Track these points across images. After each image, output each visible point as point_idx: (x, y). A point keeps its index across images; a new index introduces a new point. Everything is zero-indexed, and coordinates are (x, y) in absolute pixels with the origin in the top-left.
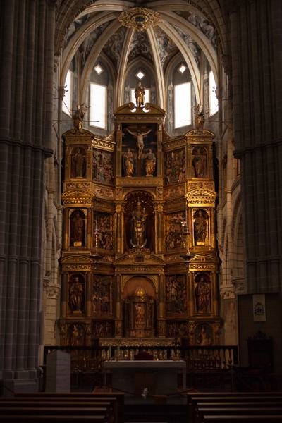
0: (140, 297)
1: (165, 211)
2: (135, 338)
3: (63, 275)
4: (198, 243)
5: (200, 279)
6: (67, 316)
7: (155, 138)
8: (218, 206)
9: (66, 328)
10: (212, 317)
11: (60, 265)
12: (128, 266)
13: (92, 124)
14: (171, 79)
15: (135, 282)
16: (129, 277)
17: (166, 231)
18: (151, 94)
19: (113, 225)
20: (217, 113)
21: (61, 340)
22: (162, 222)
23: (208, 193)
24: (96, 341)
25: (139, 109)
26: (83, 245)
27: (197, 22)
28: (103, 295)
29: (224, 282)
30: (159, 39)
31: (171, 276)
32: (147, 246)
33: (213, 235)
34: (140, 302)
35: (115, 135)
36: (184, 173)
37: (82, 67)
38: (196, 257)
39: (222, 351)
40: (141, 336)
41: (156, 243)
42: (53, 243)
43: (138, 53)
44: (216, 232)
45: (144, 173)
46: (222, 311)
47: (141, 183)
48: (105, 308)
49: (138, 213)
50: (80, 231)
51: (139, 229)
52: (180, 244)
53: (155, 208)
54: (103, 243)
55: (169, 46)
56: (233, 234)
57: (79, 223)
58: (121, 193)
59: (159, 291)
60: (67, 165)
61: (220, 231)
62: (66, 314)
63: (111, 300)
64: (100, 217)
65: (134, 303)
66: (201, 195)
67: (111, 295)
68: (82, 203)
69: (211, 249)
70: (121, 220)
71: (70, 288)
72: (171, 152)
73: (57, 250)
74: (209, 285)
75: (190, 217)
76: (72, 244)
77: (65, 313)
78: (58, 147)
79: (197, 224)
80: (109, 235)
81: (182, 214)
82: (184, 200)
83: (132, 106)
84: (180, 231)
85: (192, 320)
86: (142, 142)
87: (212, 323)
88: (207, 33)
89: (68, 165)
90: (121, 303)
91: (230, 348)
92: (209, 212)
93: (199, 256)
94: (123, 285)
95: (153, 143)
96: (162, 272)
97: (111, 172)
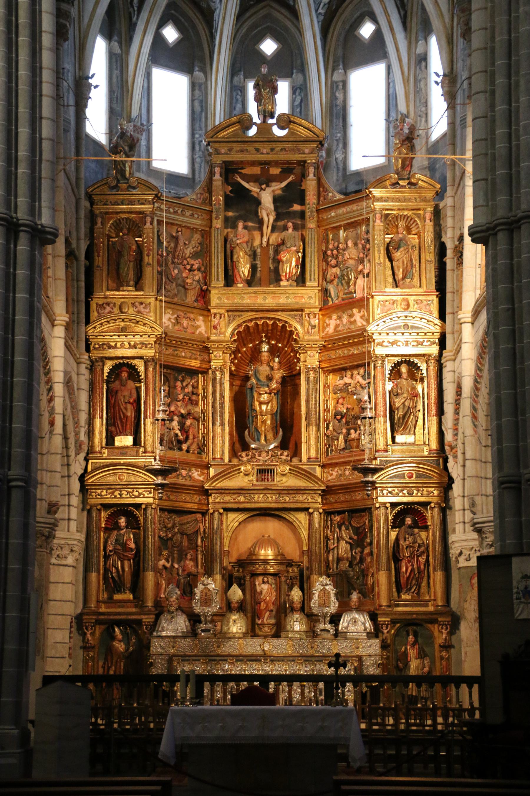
0: (266, 562)
1: (324, 365)
3: (89, 512)
4: (399, 438)
5: (403, 522)
6: (98, 607)
9: (98, 634)
12: (240, 491)
13: (156, 164)
14: (340, 52)
16: (241, 517)
17: (327, 410)
18: (294, 90)
19: (205, 397)
20: (444, 135)
21: (85, 662)
22: (317, 392)
23: (422, 324)
25: (264, 128)
26: (137, 442)
28: (181, 557)
29: (459, 528)
33: (434, 420)
34: (265, 574)
35: (209, 188)
36: (368, 275)
37: (132, 27)
38: (391, 471)
42: (66, 438)
44: (440, 412)
49: (264, 370)
50: (130, 413)
52: (359, 440)
53: (302, 357)
54: (181, 437)
56: (474, 417)
57: (126, 393)
58: (223, 323)
59: (310, 548)
61: (449, 408)
62: (98, 601)
64: (176, 379)
65: (254, 575)
66: (406, 326)
67: (200, 557)
68: (135, 347)
70: (222, 385)
71: (106, 542)
72: (338, 228)
74: (423, 534)
75: (379, 377)
76: (110, 442)
77: (94, 599)
78: (78, 219)
79: (397, 395)
80: (197, 419)
81: (362, 371)
82: (370, 340)
83: (247, 123)
85: (386, 615)
86: (272, 207)
87: (434, 621)
89: (100, 260)
90: (223, 576)
91: (470, 681)
92: (423, 367)
93: (402, 469)
94: (227, 535)
95: (297, 207)
97: (198, 276)
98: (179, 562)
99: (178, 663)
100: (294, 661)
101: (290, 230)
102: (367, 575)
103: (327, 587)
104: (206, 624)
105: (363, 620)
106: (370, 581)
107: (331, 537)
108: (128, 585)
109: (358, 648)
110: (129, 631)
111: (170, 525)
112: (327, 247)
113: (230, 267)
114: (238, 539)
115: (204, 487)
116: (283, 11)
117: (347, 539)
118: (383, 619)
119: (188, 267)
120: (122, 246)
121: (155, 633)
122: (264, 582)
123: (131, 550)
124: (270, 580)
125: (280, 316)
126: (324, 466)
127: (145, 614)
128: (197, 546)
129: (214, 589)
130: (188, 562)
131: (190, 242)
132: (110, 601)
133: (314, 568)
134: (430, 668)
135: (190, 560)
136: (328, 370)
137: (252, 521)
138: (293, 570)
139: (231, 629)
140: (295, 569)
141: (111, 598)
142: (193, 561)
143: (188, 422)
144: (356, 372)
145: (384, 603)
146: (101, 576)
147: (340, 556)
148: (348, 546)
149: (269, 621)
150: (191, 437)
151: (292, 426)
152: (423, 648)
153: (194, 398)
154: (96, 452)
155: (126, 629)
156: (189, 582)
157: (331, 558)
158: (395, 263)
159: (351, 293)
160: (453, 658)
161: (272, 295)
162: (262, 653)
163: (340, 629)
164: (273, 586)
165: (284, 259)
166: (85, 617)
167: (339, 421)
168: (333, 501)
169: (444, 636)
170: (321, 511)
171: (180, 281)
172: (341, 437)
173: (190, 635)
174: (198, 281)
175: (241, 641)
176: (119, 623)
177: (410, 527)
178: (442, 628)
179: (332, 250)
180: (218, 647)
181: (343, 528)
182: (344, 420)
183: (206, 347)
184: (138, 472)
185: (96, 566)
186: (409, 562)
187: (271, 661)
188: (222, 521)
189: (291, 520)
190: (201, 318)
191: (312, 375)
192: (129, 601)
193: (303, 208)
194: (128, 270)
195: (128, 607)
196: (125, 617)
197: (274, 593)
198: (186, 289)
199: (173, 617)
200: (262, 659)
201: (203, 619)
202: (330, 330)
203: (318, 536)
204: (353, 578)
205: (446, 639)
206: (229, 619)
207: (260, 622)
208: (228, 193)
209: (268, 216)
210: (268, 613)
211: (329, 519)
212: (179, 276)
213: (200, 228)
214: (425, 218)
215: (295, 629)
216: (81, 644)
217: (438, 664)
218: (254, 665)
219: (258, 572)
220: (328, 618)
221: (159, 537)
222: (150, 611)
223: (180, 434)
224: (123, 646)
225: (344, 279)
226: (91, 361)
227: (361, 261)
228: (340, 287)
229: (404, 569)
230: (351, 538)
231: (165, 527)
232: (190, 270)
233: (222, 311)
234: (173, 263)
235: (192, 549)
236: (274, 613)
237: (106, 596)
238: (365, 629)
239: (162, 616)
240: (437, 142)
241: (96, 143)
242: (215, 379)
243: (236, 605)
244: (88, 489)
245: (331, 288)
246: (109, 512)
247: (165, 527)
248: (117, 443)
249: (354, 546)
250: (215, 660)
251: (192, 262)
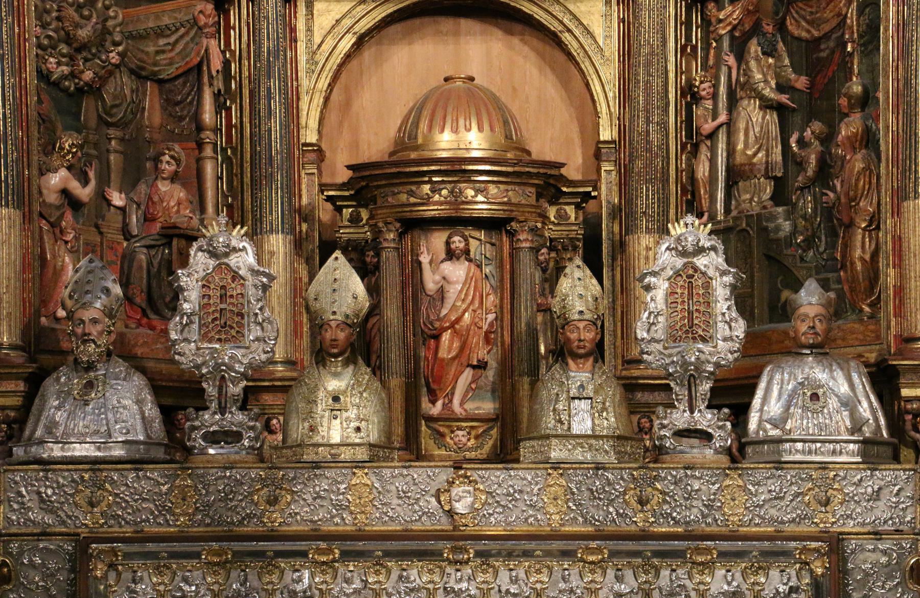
67: (209, 169)
98: (129, 185)
99: (112, 566)
100: (567, 554)
102: (850, 225)
103: (701, 262)
104: (222, 410)
105: (844, 388)
106: (859, 251)
107: (705, 89)
109: (827, 503)
114: (355, 107)
117: (767, 92)
121: (19, 452)
122: (451, 255)
124: (474, 244)
128: (200, 128)
129: (255, 273)
133: (641, 204)
135: (174, 178)
138: (562, 217)
139: (323, 431)
140: (570, 210)
142: (184, 185)
147: (739, 159)
148: (772, 118)
149: (469, 406)
157: (702, 170)
162: (444, 524)
163: (753, 425)
164: (487, 270)
173: (160, 454)
175: (361, 478)
180: (273, 501)
181: (754, 47)
187: (478, 554)
188: (293, 30)
189: (554, 26)
197: (491, 300)
199: (90, 385)
200: (445, 547)
201: (210, 389)
203: (657, 83)
204: (789, 241)
206: (316, 389)
207: (436, 409)
211: (696, 18)
215: (576, 429)
218: (413, 574)
219: (432, 211)
220: (705, 387)
221: (43, 76)
230: (781, 88)
231: (68, 39)
236: (490, 374)
238: (856, 428)
239: (48, 382)
243: (341, 336)
249: (797, 119)
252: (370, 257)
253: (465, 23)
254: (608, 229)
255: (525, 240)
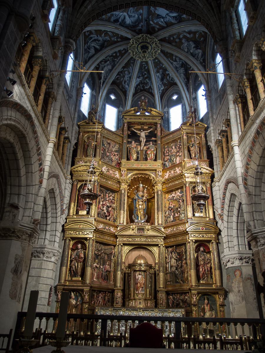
0: (140, 265)
2: (134, 309)
4: (197, 215)
5: (199, 250)
7: (155, 136)
8: (214, 180)
10: (214, 287)
11: (63, 231)
12: (130, 236)
15: (136, 253)
16: (131, 248)
24: (93, 310)
26: (88, 213)
27: (188, 49)
28: (104, 264)
30: (158, 74)
31: (171, 247)
32: (147, 221)
34: (140, 271)
39: (232, 324)
40: (142, 306)
41: (156, 218)
43: (142, 88)
45: (146, 159)
46: (225, 280)
47: (144, 167)
48: (106, 277)
51: (141, 206)
55: (165, 81)
59: (159, 261)
60: (79, 147)
62: (65, 280)
63: (112, 269)
64: (106, 193)
69: (210, 219)
73: (62, 213)
76: (77, 213)
81: (179, 191)
84: (177, 206)
85: (195, 290)
86: (145, 137)
88: (196, 57)
90: (122, 273)
95: (153, 139)
96: (161, 242)
97: (117, 157)
98: (103, 265)
101: (151, 144)
102: (185, 273)
108: (80, 274)
110: (78, 295)
111: (99, 249)
112: (165, 151)
113: (129, 154)
115: (115, 234)
116: (148, 94)
118: (194, 292)
119: (113, 154)
120: (89, 143)
122: (139, 274)
123: (82, 258)
125: (147, 172)
126: (164, 228)
127: (85, 287)
130: (107, 266)
131: (115, 147)
132: (71, 281)
134: (215, 316)
136: (165, 192)
137: (135, 251)
140: (153, 270)
141: (72, 279)
142: (109, 266)
143: (110, 209)
144: (177, 191)
145: (194, 284)
146: (68, 269)
150: (111, 215)
151: (150, 217)
152: (212, 307)
153: (113, 201)
154: (71, 216)
155: (77, 293)
156: (107, 274)
158: (191, 152)
159: (174, 163)
160: (226, 311)
161: (144, 164)
165: (149, 153)
166: (58, 287)
167: (170, 211)
168: (168, 241)
169: (221, 300)
170: (164, 245)
171: (110, 158)
172: (172, 216)
174: (117, 159)
176: (73, 291)
177: (202, 252)
178: (220, 297)
179: (166, 151)
182: (172, 211)
183: (119, 181)
184: (87, 224)
185: (66, 264)
186: (203, 266)
190: (117, 172)
191: (160, 193)
192: (79, 281)
193: (156, 139)
194: (90, 151)
195: (78, 284)
196: (76, 287)
198: (112, 161)
202: (167, 177)
205: (222, 302)
208: (129, 134)
209: (143, 139)
210: (141, 288)
212: (110, 156)
213: (119, 142)
214: (202, 136)
216: (56, 300)
217: (219, 314)
219: (137, 269)
222: (87, 285)
223: (106, 213)
224: (75, 302)
225: (171, 159)
226: (73, 181)
227: (178, 152)
228: (170, 163)
229: (201, 270)
231: (98, 250)
232: (114, 155)
233: (126, 170)
234: (108, 152)
235: (109, 261)
237: (70, 279)
240: (202, 118)
241: (84, 115)
242: (122, 193)
244: (65, 231)
245: (167, 163)
246: (74, 242)
247: (98, 250)
248: (80, 213)
250: (116, 309)
251: (115, 153)
252: (130, 274)
253: (141, 249)
254: (157, 272)
255: (148, 273)
